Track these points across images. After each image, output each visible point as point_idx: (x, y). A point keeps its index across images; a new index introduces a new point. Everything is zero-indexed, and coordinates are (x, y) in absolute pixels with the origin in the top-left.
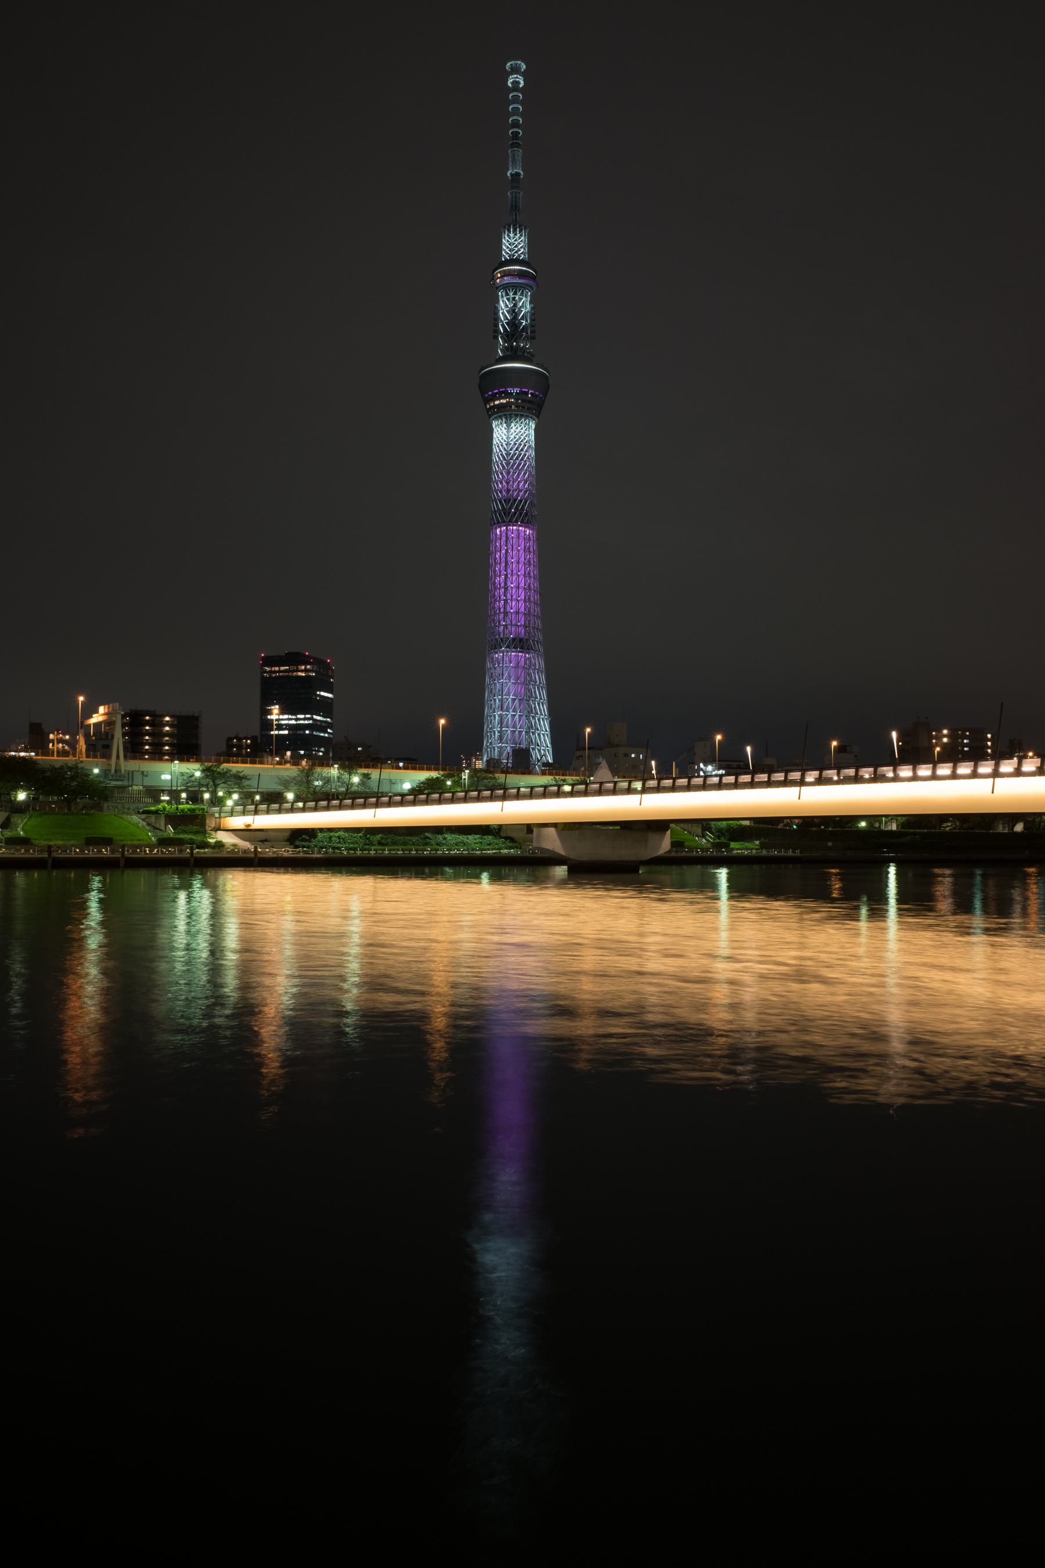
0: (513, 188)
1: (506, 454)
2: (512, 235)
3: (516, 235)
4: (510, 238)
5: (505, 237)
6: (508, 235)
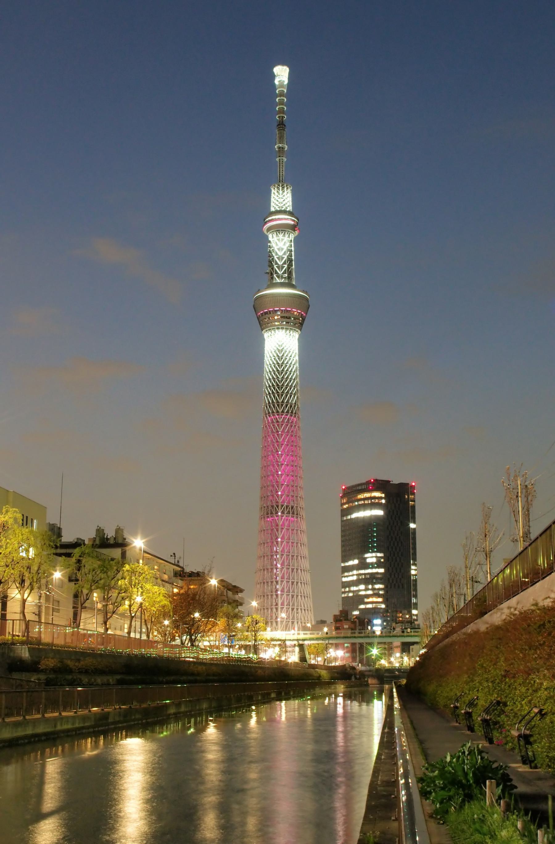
0: (280, 157)
1: (279, 359)
2: (281, 192)
3: (284, 192)
4: (279, 194)
5: (274, 193)
6: (277, 192)
